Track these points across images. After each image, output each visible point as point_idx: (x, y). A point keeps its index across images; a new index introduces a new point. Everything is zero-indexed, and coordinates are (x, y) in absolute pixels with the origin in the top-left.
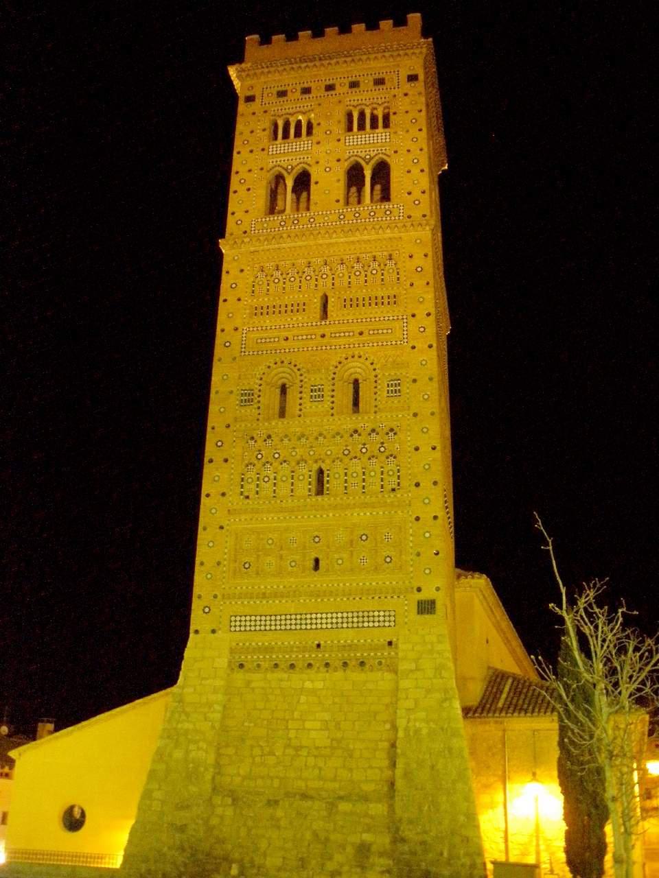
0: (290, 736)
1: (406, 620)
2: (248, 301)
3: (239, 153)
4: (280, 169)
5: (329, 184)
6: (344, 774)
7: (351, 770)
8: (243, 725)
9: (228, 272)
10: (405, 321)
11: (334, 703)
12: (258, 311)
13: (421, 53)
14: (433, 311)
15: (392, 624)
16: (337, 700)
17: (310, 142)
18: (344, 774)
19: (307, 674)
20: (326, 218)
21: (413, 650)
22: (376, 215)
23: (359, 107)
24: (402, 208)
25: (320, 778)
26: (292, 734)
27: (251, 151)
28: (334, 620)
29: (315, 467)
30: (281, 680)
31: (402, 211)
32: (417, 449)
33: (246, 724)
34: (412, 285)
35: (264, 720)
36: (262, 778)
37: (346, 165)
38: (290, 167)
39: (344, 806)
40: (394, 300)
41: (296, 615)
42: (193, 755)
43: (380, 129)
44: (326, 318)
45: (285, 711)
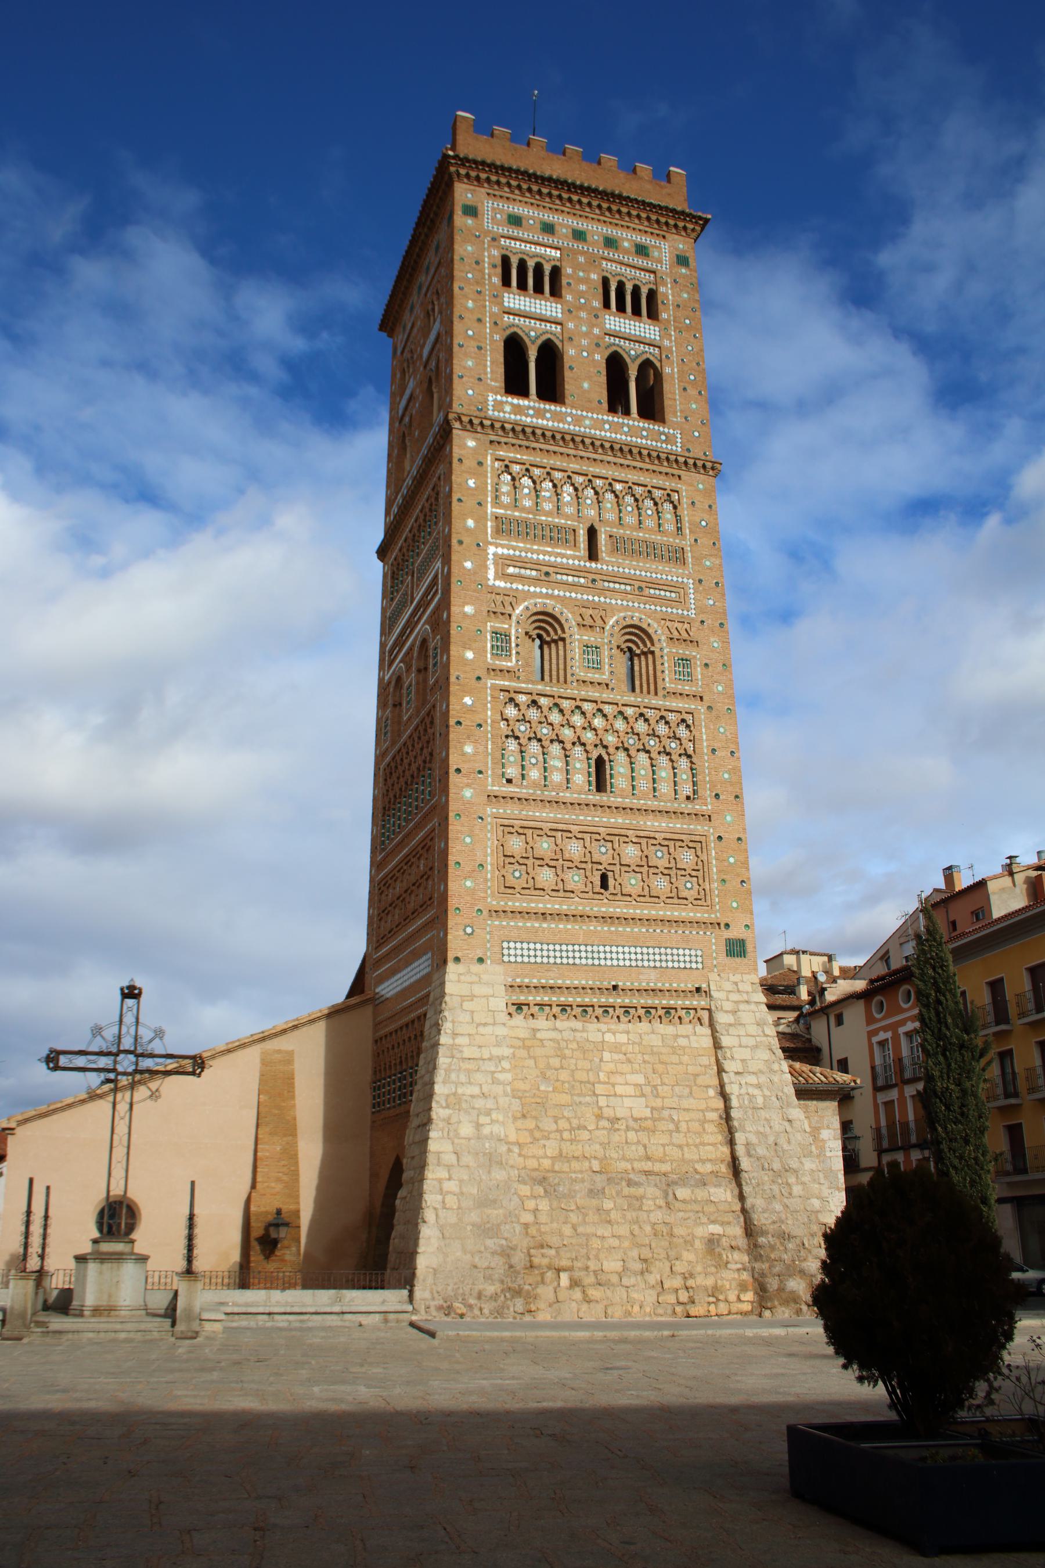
0: (600, 1104)
1: (715, 962)
5: (584, 376)
6: (674, 1153)
7: (680, 1147)
8: (538, 1089)
9: (460, 460)
11: (644, 1062)
13: (693, 230)
15: (700, 966)
16: (646, 1057)
18: (675, 1153)
19: (605, 1023)
21: (728, 1000)
23: (618, 278)
25: (648, 1158)
26: (602, 1101)
28: (633, 957)
29: (595, 755)
30: (574, 1030)
32: (714, 751)
33: (542, 1088)
34: (696, 540)
35: (563, 1082)
36: (577, 1158)
37: (607, 354)
39: (682, 1193)
40: (677, 556)
41: (586, 945)
42: (486, 1131)
45: (588, 1071)
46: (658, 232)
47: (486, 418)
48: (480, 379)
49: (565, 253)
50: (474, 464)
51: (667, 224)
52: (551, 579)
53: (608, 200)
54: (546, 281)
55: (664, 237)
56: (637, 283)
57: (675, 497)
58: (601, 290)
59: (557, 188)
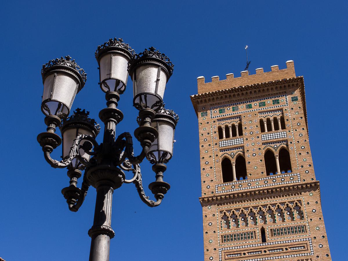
2: (219, 233)
3: (203, 146)
4: (228, 156)
5: (255, 164)
9: (206, 216)
10: (310, 241)
12: (225, 238)
13: (297, 84)
14: (325, 235)
17: (242, 139)
20: (257, 183)
22: (285, 181)
23: (267, 117)
24: (299, 175)
27: (210, 145)
31: (299, 177)
34: (311, 219)
38: (232, 154)
40: (302, 229)
43: (280, 130)
44: (265, 241)
46: (282, 91)
47: (214, 197)
48: (212, 180)
49: (242, 117)
50: (211, 215)
51: (285, 86)
52: (246, 256)
53: (258, 88)
54: (237, 130)
55: (285, 92)
56: (275, 116)
57: (299, 204)
58: (259, 126)
59: (236, 92)
